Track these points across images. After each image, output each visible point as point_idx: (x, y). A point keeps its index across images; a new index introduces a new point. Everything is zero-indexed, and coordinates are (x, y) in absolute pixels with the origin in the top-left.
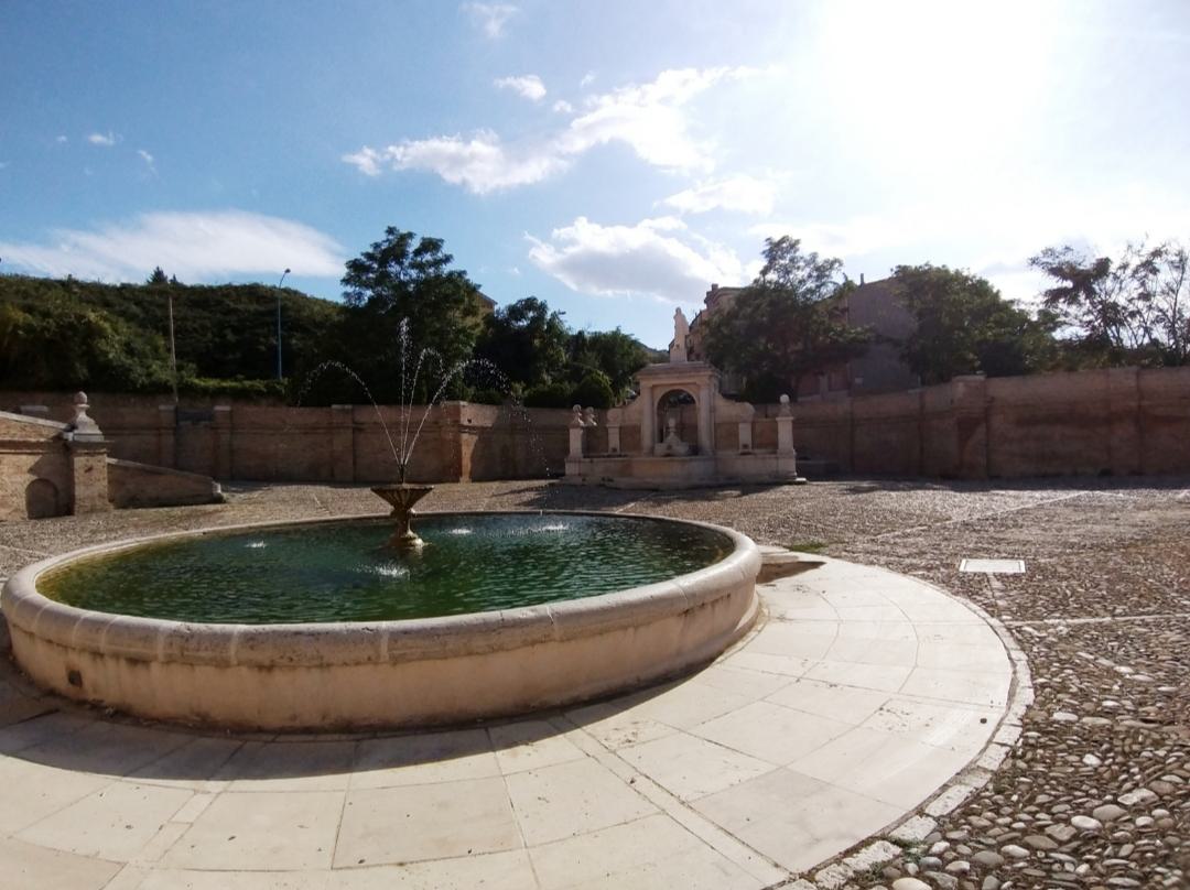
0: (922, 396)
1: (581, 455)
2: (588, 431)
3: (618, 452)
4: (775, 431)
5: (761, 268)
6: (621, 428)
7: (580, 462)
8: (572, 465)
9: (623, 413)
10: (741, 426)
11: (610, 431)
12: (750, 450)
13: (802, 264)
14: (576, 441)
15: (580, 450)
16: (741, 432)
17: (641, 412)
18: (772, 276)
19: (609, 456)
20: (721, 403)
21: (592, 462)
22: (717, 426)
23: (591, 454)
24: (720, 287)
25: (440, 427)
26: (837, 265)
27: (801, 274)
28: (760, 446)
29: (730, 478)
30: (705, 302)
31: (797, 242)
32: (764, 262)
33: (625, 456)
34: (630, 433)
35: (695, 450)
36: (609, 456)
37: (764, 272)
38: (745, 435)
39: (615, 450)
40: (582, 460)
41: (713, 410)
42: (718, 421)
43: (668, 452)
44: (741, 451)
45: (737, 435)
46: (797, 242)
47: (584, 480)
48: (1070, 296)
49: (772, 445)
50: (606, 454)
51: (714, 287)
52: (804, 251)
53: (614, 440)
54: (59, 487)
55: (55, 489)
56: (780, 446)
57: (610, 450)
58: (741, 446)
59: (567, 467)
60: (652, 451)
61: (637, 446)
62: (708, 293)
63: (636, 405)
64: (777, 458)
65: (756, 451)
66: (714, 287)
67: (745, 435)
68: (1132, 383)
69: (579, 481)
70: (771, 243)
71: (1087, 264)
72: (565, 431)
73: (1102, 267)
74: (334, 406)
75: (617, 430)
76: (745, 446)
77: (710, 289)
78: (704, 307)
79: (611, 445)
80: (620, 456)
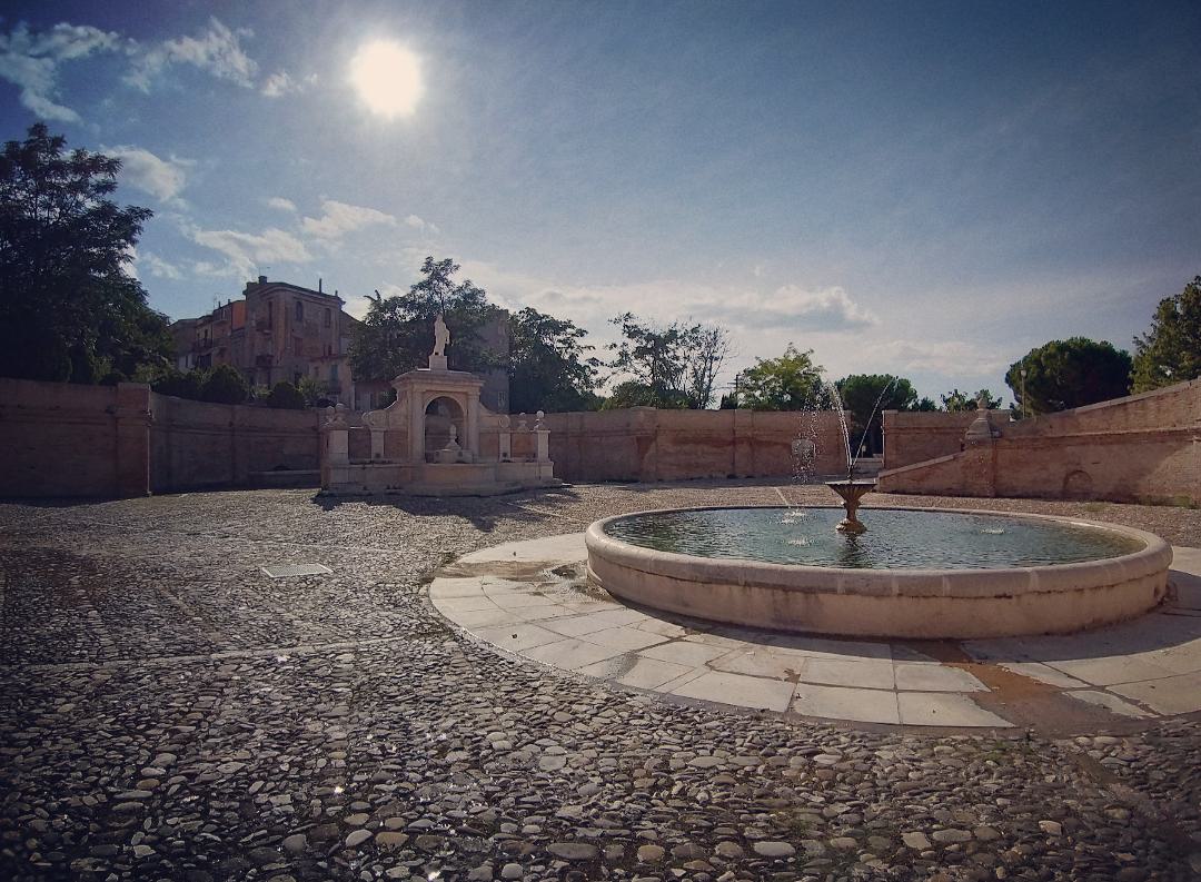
0: (582, 417)
14: (339, 444)
20: (484, 412)
22: (480, 434)
28: (519, 455)
29: (516, 483)
30: (244, 293)
32: (425, 277)
33: (389, 463)
34: (396, 439)
36: (371, 462)
37: (421, 286)
38: (505, 445)
39: (378, 456)
41: (479, 419)
43: (461, 459)
44: (502, 458)
47: (365, 489)
48: (640, 353)
49: (532, 456)
50: (367, 460)
51: (263, 279)
53: (378, 445)
57: (373, 455)
60: (428, 458)
63: (400, 409)
64: (540, 466)
65: (513, 459)
66: (263, 279)
67: (505, 445)
68: (749, 420)
71: (660, 330)
72: (319, 436)
73: (672, 335)
76: (505, 455)
79: (375, 450)
80: (384, 463)
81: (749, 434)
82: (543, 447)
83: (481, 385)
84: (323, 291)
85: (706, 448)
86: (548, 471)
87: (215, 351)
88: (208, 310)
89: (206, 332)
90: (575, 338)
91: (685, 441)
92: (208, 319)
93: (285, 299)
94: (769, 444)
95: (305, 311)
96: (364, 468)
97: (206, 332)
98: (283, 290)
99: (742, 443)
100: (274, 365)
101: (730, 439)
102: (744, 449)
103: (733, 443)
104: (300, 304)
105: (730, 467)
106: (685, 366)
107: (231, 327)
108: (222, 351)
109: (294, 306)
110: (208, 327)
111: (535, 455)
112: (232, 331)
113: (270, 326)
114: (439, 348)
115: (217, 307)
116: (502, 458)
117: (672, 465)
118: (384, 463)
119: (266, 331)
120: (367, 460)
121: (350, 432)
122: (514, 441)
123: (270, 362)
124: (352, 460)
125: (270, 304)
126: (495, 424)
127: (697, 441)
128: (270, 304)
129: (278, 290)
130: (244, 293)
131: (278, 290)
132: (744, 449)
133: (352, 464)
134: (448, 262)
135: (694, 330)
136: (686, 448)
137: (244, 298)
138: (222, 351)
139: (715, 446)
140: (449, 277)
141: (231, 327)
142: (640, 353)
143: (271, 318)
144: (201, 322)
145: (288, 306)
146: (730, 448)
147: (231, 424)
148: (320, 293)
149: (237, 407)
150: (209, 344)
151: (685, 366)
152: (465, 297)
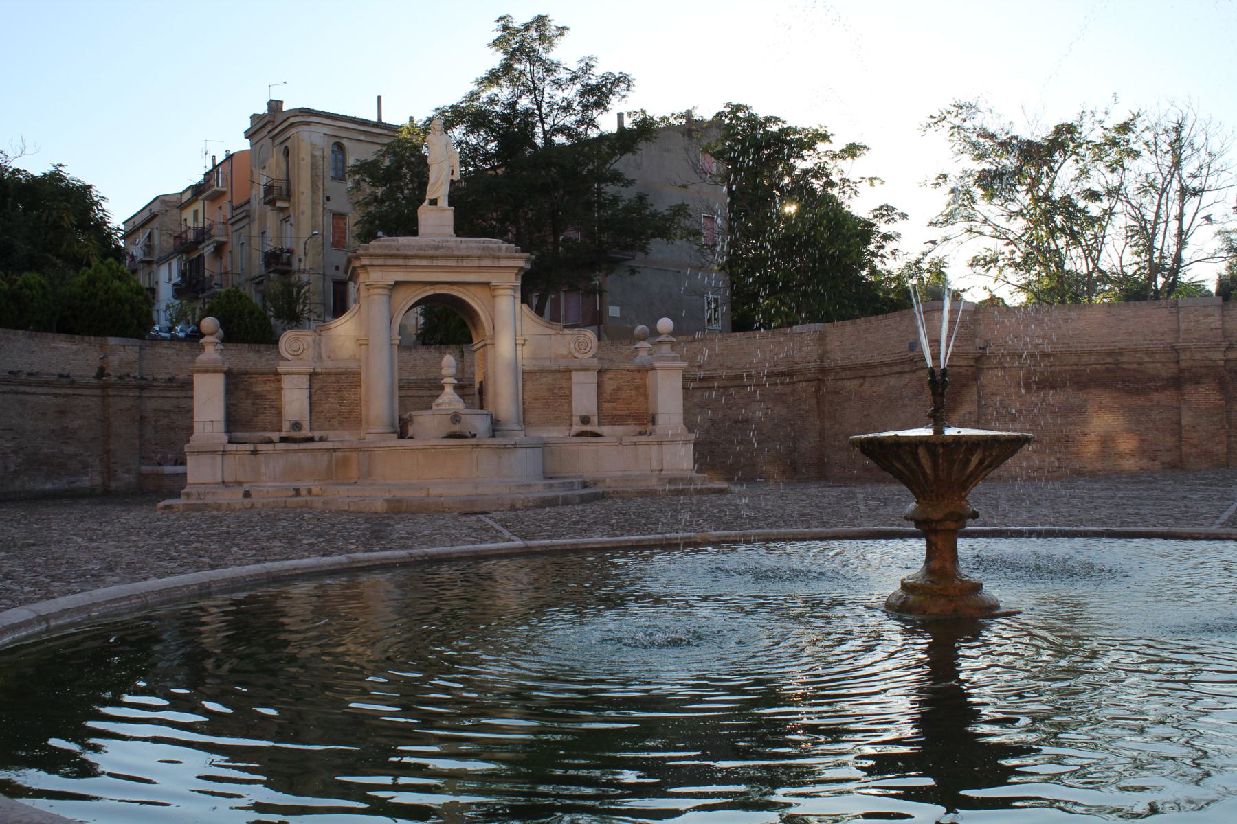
1: (225, 438)
2: (235, 382)
3: (306, 432)
4: (643, 391)
5: (483, 73)
6: (313, 375)
7: (224, 453)
8: (206, 459)
9: (317, 344)
10: (574, 375)
11: (287, 382)
12: (595, 429)
13: (563, 75)
15: (221, 427)
16: (576, 391)
18: (503, 92)
19: (284, 440)
21: (255, 452)
23: (239, 435)
24: (285, 108)
26: (623, 86)
27: (559, 95)
28: (615, 420)
29: (585, 485)
31: (562, 30)
32: (496, 59)
33: (321, 440)
35: (496, 427)
36: (284, 440)
37: (492, 78)
38: (584, 397)
39: (297, 426)
40: (233, 447)
43: (456, 428)
44: (578, 428)
46: (562, 30)
47: (247, 494)
48: (992, 182)
49: (646, 420)
50: (275, 436)
51: (275, 105)
52: (566, 54)
56: (661, 419)
57: (286, 426)
58: (576, 419)
59: (190, 460)
60: (402, 430)
61: (352, 417)
62: (254, 117)
65: (605, 430)
66: (275, 105)
67: (584, 397)
69: (233, 497)
70: (505, 28)
75: (306, 378)
76: (585, 420)
77: (263, 109)
80: (311, 440)
81: (1218, 356)
83: (522, 264)
84: (384, 120)
86: (681, 459)
87: (208, 250)
88: (198, 178)
89: (196, 212)
90: (841, 163)
92: (197, 190)
93: (311, 139)
96: (255, 452)
97: (196, 212)
98: (308, 123)
99: (1197, 379)
100: (295, 266)
101: (1166, 371)
103: (1176, 382)
105: (1170, 441)
106: (1110, 212)
107: (231, 201)
108: (219, 249)
109: (328, 152)
110: (199, 205)
111: (653, 421)
112: (234, 209)
113: (288, 196)
114: (439, 186)
115: (210, 167)
118: (311, 440)
119: (279, 204)
120: (275, 436)
121: (229, 374)
122: (609, 386)
123: (289, 263)
125: (287, 152)
126: (564, 351)
128: (287, 152)
129: (292, 125)
130: (249, 135)
131: (292, 125)
133: (230, 442)
134: (541, 21)
135: (1125, 128)
136: (1052, 397)
137: (246, 145)
138: (219, 249)
140: (554, 55)
141: (231, 201)
142: (992, 182)
143: (288, 181)
144: (188, 195)
145: (318, 153)
147: (101, 373)
148: (379, 124)
149: (112, 341)
150: (202, 235)
151: (1110, 212)
152: (588, 90)
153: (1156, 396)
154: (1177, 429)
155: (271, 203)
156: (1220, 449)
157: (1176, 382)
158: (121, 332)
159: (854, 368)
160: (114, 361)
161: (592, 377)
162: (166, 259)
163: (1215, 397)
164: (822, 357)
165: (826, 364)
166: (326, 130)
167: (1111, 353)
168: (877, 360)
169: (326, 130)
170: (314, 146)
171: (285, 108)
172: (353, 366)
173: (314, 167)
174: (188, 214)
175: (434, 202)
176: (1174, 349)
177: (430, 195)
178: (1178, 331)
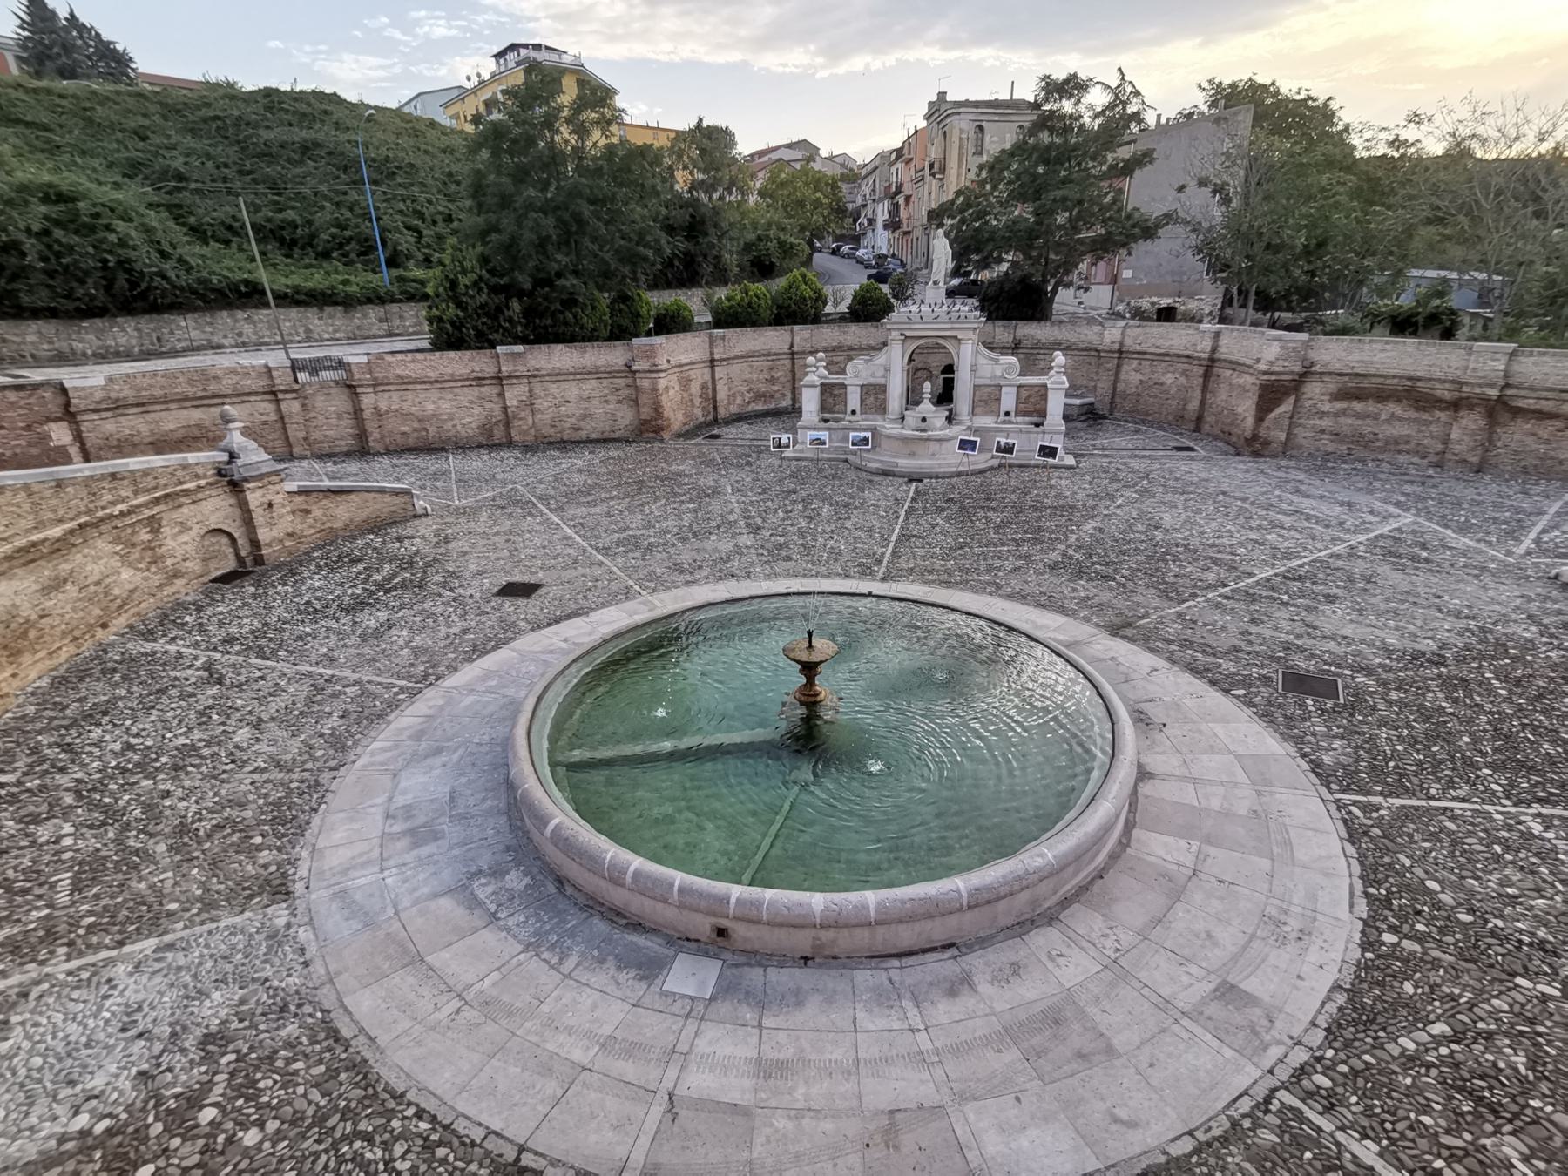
0: (1217, 334)
2: (826, 387)
17: (887, 370)
24: (949, 98)
25: (635, 372)
41: (974, 369)
42: (979, 382)
45: (999, 400)
49: (1042, 414)
54: (236, 535)
55: (229, 535)
61: (882, 409)
63: (881, 359)
65: (1020, 419)
66: (942, 95)
67: (1008, 401)
74: (499, 348)
76: (1007, 414)
77: (935, 98)
78: (923, 124)
82: (1056, 405)
85: (1397, 409)
87: (901, 199)
91: (1359, 395)
92: (899, 152)
94: (1541, 415)
95: (987, 138)
99: (1471, 408)
102: (1472, 421)
104: (981, 128)
108: (908, 199)
109: (972, 134)
113: (943, 170)
116: (1002, 418)
117: (1323, 431)
124: (827, 415)
127: (1383, 394)
130: (927, 118)
132: (1472, 421)
136: (1357, 406)
137: (924, 124)
138: (908, 199)
139: (1418, 409)
146: (1442, 416)
147: (792, 346)
149: (796, 328)
153: (1438, 414)
154: (1446, 441)
155: (933, 175)
156: (1475, 460)
157: (1455, 405)
158: (804, 320)
159: (1231, 362)
160: (797, 339)
161: (1014, 390)
162: (881, 200)
163: (1482, 423)
164: (1214, 350)
165: (1217, 356)
166: (972, 117)
167: (1410, 379)
168: (1243, 361)
169: (972, 117)
170: (962, 131)
171: (949, 98)
172: (882, 381)
173: (961, 147)
174: (893, 170)
175: (935, 283)
176: (1462, 384)
177: (934, 278)
178: (1467, 368)
